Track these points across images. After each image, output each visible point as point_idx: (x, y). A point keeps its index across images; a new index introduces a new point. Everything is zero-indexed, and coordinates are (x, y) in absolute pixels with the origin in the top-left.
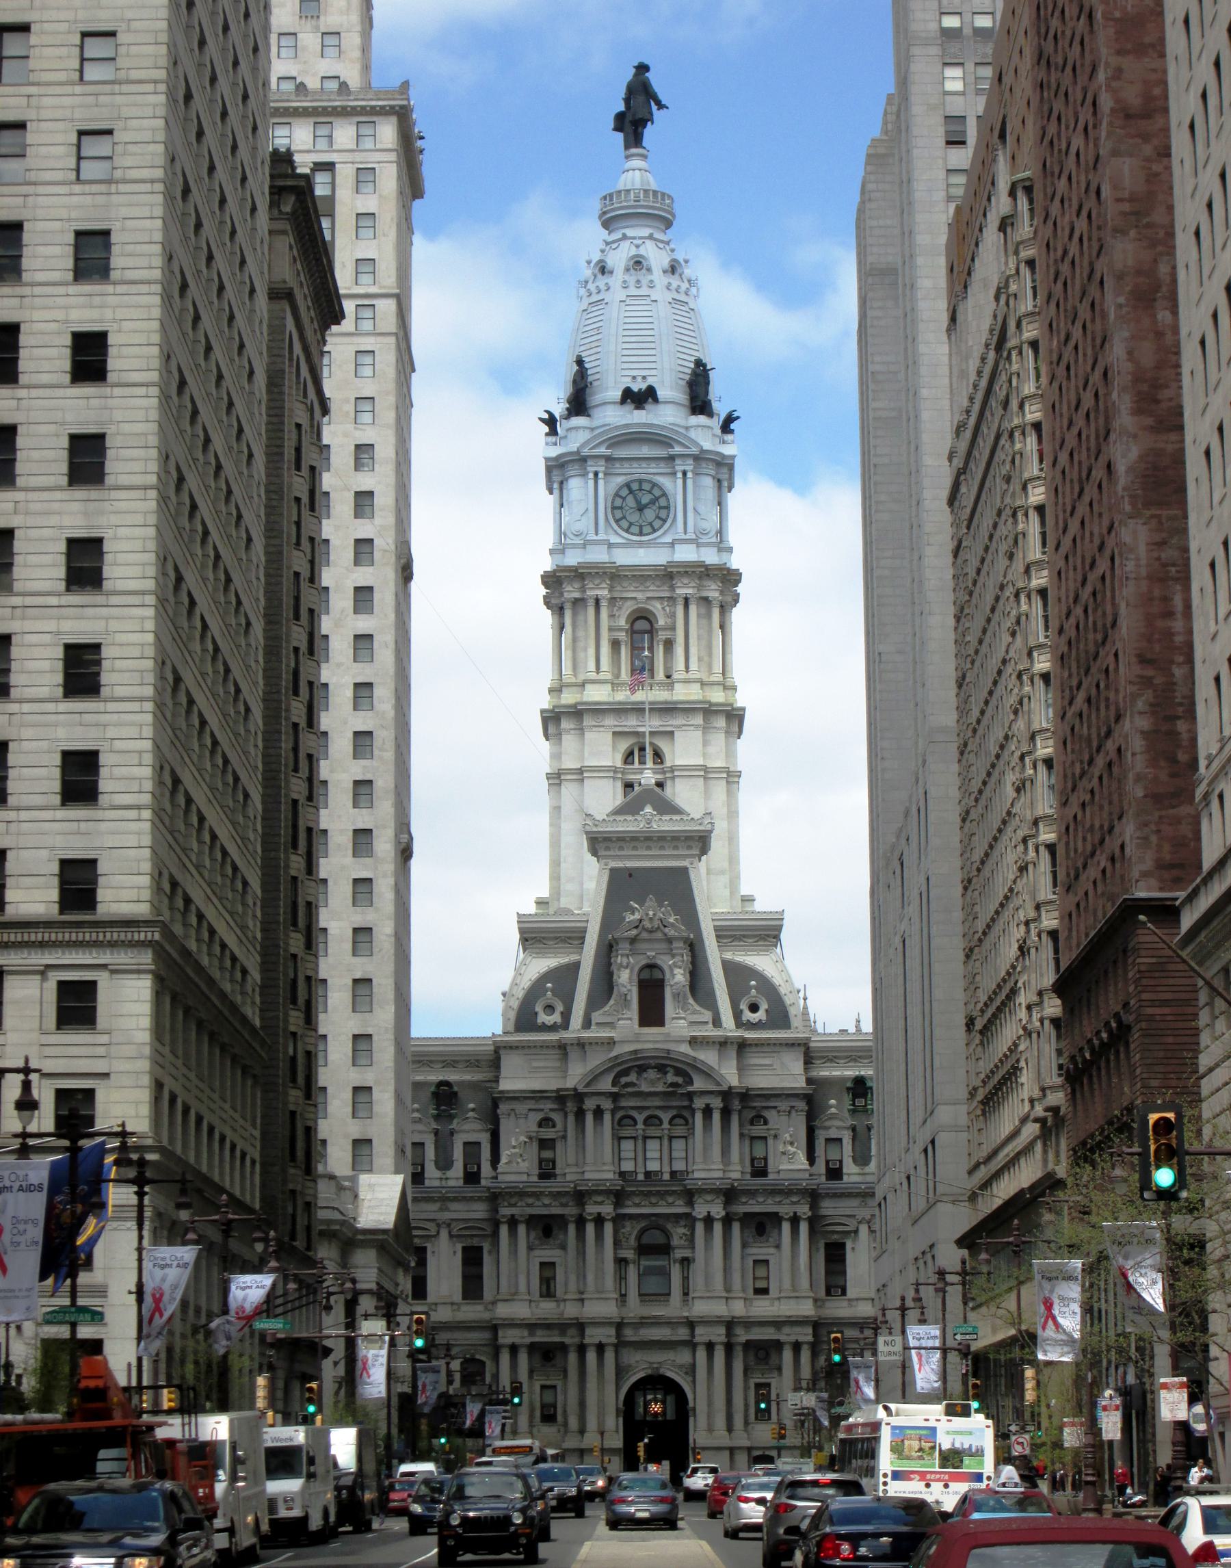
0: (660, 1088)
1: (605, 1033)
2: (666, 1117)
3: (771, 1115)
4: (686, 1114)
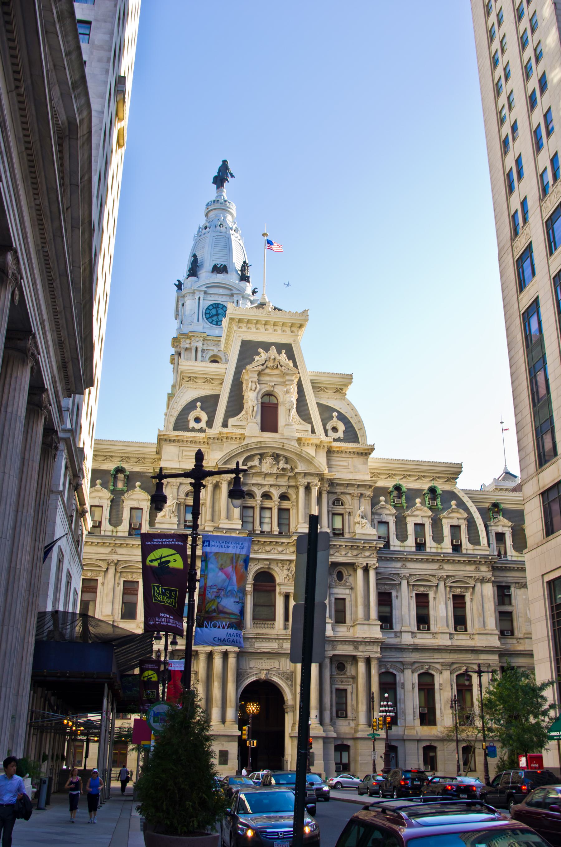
0: (275, 470)
1: (239, 431)
2: (276, 494)
3: (347, 499)
4: (291, 492)
